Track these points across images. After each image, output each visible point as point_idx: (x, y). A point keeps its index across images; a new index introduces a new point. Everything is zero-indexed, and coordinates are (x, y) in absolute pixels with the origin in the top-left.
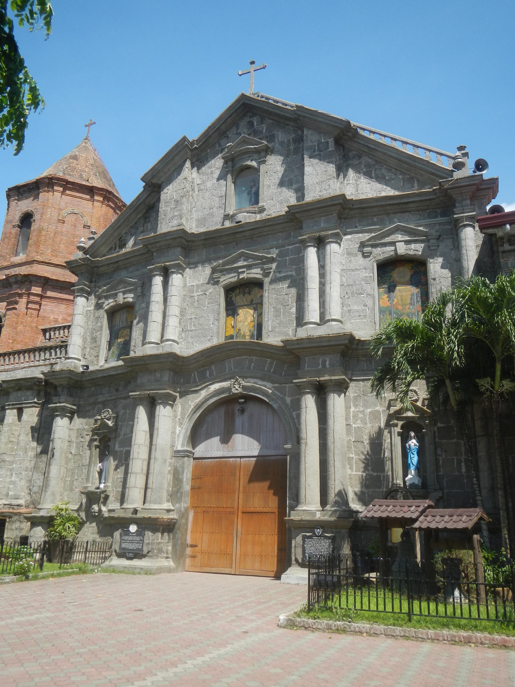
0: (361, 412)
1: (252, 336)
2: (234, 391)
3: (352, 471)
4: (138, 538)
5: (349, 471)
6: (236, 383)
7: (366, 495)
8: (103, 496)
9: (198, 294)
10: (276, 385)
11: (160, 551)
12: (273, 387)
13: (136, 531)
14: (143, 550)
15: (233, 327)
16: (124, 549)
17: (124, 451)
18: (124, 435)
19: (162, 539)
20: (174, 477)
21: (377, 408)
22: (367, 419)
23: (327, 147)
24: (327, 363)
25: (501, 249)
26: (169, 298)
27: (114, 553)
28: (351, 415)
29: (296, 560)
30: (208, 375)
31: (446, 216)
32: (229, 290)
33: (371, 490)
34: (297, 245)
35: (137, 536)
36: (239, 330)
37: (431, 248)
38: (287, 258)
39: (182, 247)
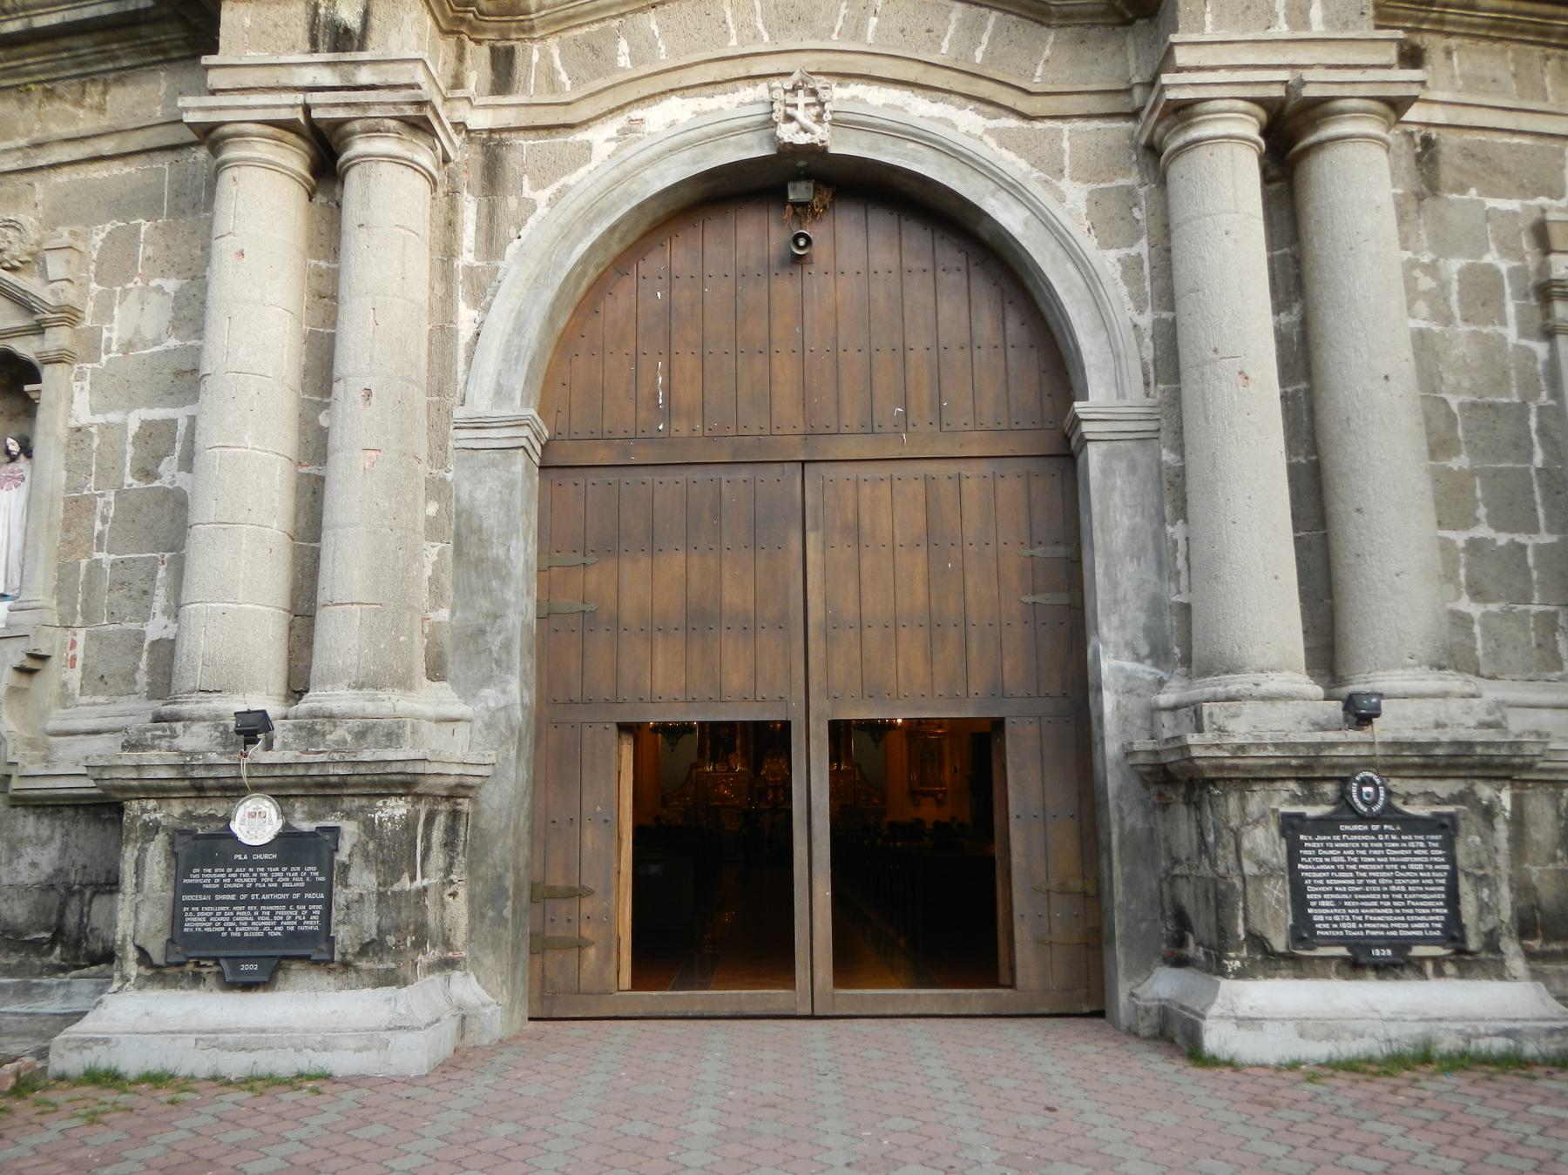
2: (788, 134)
4: (295, 877)
6: (802, 99)
7: (1477, 629)
10: (1012, 122)
12: (987, 131)
13: (279, 836)
14: (331, 941)
17: (133, 426)
18: (128, 346)
19: (423, 877)
20: (458, 551)
22: (1454, 298)
27: (132, 969)
29: (1257, 942)
30: (624, 61)
33: (1493, 608)
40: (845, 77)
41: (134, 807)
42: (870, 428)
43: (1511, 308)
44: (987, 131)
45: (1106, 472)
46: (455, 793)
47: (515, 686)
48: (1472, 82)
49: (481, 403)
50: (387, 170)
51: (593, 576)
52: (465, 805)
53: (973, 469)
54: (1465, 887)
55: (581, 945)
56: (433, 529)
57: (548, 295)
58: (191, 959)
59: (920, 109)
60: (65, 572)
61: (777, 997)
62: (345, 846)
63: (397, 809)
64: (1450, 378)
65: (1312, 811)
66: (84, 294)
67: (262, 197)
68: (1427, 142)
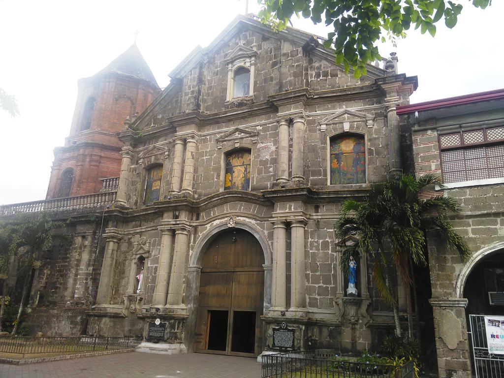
0: (315, 242)
1: (243, 188)
2: (229, 226)
3: (309, 283)
4: (161, 329)
5: (307, 284)
6: (231, 220)
8: (138, 298)
9: (207, 157)
11: (176, 338)
15: (230, 181)
16: (151, 336)
18: (154, 256)
19: (177, 330)
21: (327, 240)
23: (298, 55)
24: (293, 207)
25: (413, 129)
26: (186, 160)
28: (309, 244)
29: (269, 346)
30: (212, 215)
31: (380, 103)
32: (229, 154)
34: (275, 124)
35: (160, 327)
36: (235, 183)
37: (368, 127)
38: (268, 133)
39: (196, 124)
40: (238, 216)
41: (146, 319)
42: (242, 267)
43: (330, 248)
44: (256, 223)
45: (267, 275)
46: (183, 319)
47: (192, 305)
48: (327, 210)
49: (191, 265)
50: (180, 235)
51: (206, 288)
52: (185, 321)
53: (255, 273)
54: (295, 340)
55: (200, 342)
56: (184, 282)
57: (200, 249)
58: (150, 339)
59: (247, 220)
60: (146, 286)
61: (224, 352)
62: (167, 325)
63: (172, 321)
64: (318, 260)
65: (277, 328)
66: (150, 249)
67: (166, 239)
68: (318, 221)
